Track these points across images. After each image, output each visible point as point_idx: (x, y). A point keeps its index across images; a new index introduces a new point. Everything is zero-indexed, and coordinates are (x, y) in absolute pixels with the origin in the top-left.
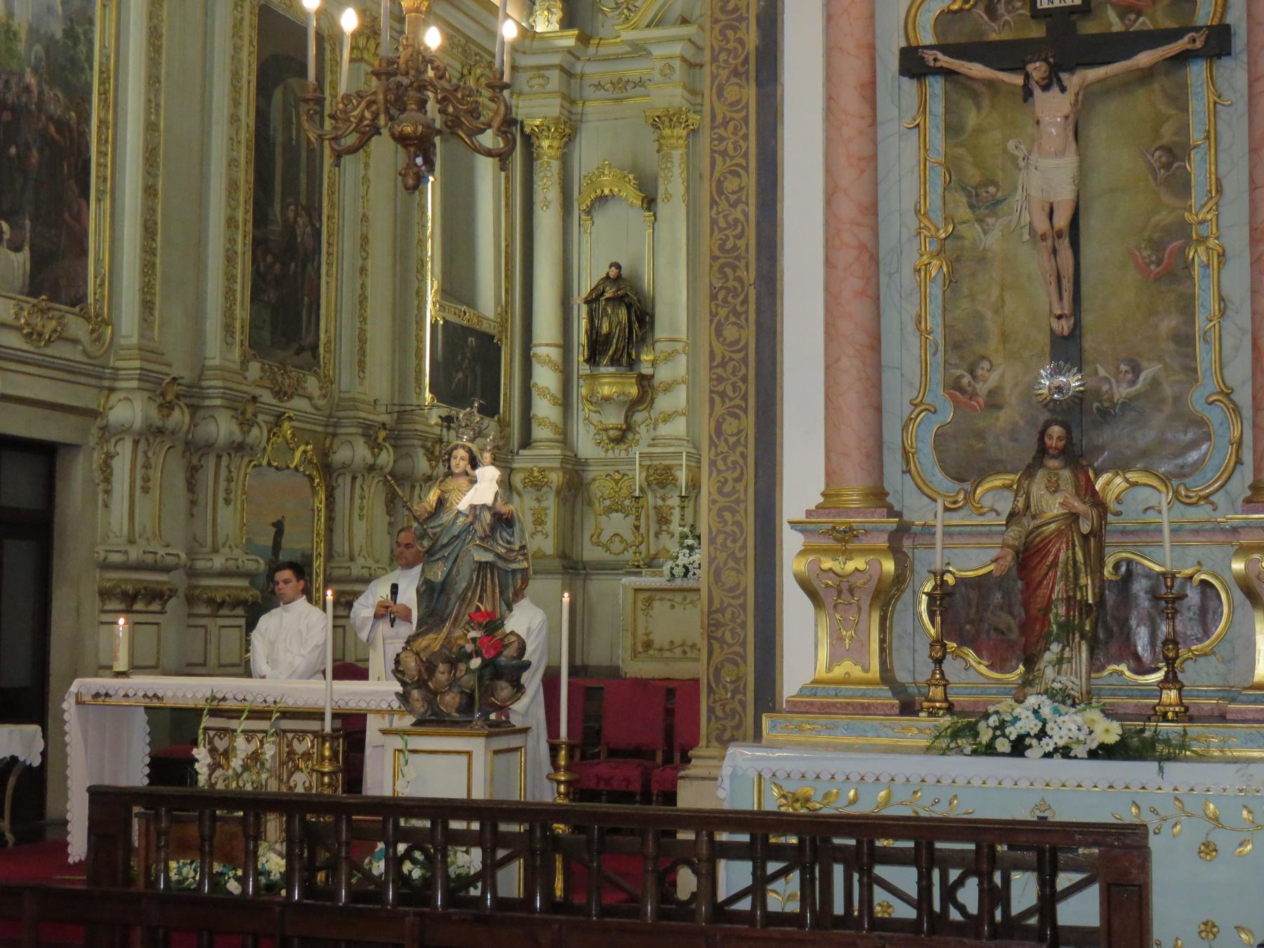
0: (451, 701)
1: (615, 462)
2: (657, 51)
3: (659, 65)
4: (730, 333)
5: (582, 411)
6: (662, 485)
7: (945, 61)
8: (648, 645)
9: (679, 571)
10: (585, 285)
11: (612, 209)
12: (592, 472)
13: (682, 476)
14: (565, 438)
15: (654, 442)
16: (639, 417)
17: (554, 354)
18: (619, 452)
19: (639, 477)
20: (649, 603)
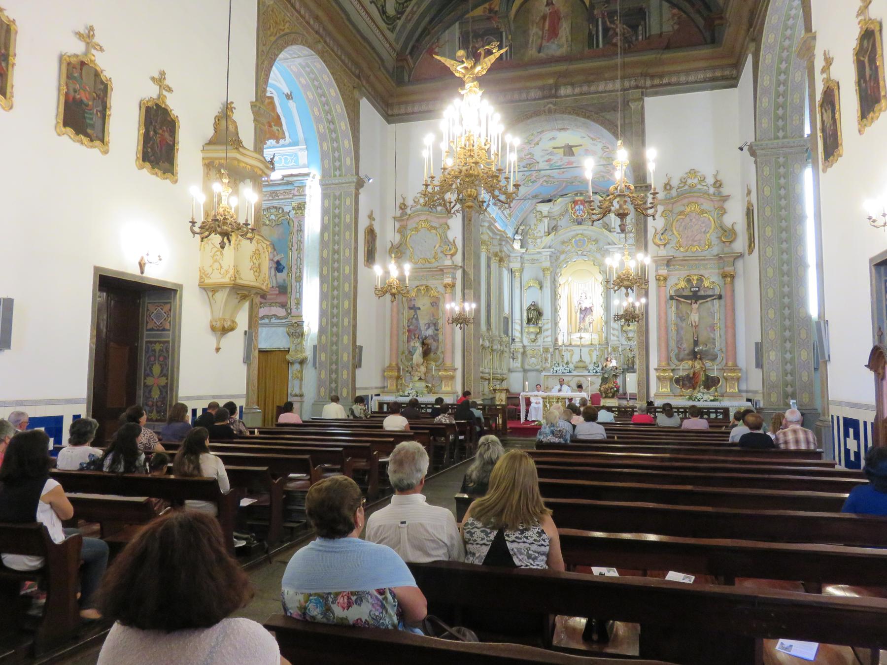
0: (610, 395)
1: (533, 346)
2: (544, 254)
3: (544, 257)
4: (641, 338)
5: (525, 335)
6: (547, 352)
7: (677, 298)
8: (547, 388)
9: (555, 371)
10: (525, 307)
11: (532, 289)
12: (527, 349)
13: (551, 350)
14: (522, 342)
15: (544, 342)
16: (538, 336)
17: (519, 322)
18: (533, 344)
19: (541, 350)
20: (547, 378)
